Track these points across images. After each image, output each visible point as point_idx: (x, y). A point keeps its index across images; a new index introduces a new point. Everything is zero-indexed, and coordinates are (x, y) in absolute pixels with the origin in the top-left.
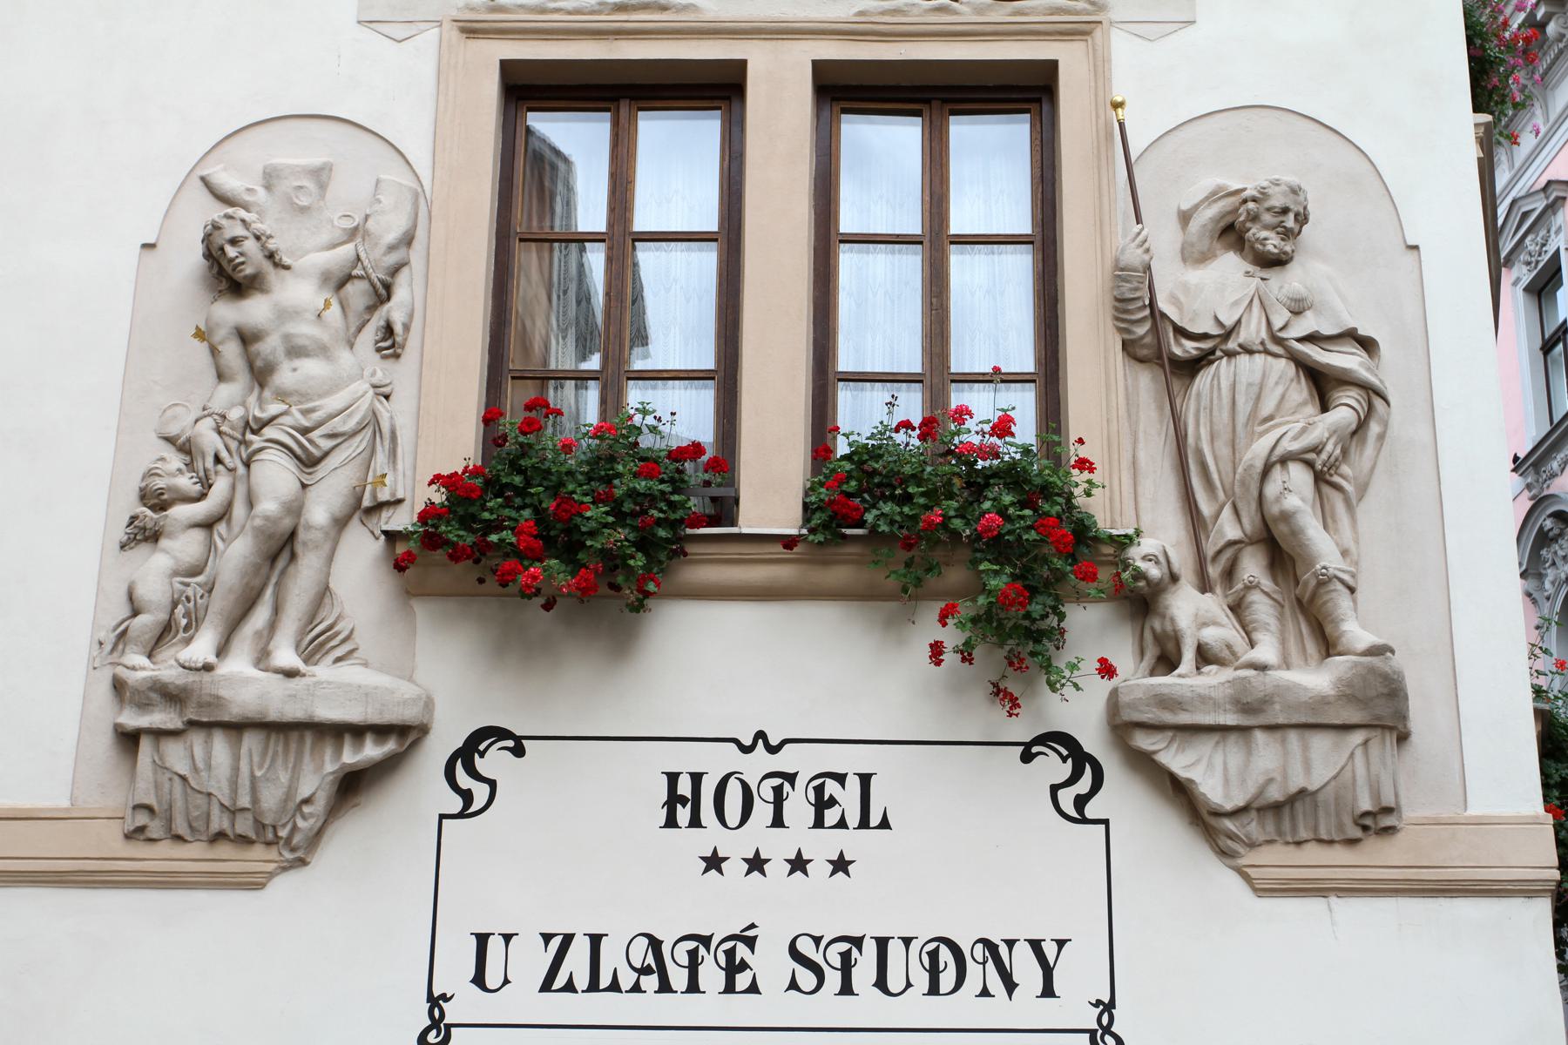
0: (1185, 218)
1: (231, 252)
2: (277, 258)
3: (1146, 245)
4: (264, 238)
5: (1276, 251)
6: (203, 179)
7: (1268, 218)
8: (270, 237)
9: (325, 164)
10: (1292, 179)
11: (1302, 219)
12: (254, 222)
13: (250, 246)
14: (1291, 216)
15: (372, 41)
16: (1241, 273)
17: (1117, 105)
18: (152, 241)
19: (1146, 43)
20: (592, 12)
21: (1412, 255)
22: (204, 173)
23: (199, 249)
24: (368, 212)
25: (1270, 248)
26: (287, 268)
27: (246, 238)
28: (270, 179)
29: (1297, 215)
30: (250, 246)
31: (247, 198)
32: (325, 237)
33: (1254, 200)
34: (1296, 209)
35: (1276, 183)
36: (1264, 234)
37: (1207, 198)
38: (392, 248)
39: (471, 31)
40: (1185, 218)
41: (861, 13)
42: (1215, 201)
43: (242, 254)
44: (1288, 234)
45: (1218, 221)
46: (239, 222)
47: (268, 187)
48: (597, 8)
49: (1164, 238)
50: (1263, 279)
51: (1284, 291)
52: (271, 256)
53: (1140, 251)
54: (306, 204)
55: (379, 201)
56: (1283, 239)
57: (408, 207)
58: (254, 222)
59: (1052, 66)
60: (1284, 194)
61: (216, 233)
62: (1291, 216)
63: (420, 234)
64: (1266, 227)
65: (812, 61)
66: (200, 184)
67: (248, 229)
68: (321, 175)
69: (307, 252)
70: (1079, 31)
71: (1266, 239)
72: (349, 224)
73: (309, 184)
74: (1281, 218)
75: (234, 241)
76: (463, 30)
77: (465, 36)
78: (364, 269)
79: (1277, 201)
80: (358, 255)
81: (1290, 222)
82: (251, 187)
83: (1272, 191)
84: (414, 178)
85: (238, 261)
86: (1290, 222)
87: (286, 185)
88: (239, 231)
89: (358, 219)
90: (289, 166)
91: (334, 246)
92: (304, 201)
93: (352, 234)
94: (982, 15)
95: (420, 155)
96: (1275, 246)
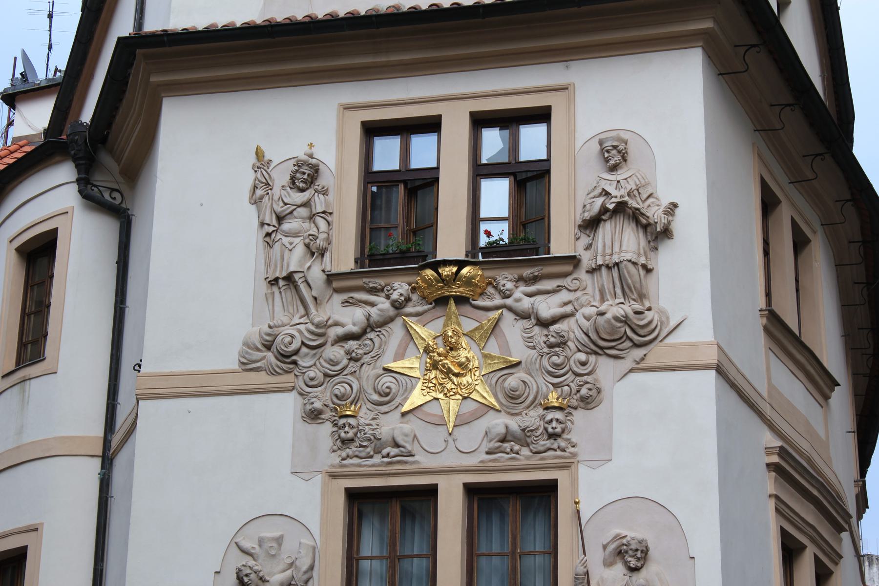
0: (605, 547)
1: (246, 580)
2: (263, 579)
3: (585, 565)
4: (258, 572)
5: (634, 566)
6: (236, 543)
7: (631, 553)
8: (260, 571)
9: (281, 536)
10: (639, 536)
11: (646, 552)
12: (254, 566)
13: (253, 576)
14: (639, 552)
15: (297, 481)
16: (622, 575)
17: (577, 503)
18: (218, 571)
19: (593, 470)
20: (379, 466)
21: (691, 561)
22: (237, 541)
23: (235, 575)
24: (297, 557)
25: (632, 565)
26: (268, 581)
27: (251, 573)
28: (261, 542)
29: (642, 551)
30: (253, 576)
31: (253, 551)
32: (281, 567)
33: (626, 545)
34: (641, 549)
35: (633, 539)
36: (630, 559)
37: (612, 539)
38: (305, 572)
39: (334, 476)
40: (605, 547)
41: (481, 462)
42: (615, 541)
43: (250, 580)
44: (638, 559)
45: (617, 549)
46: (248, 568)
47: (260, 546)
48: (381, 463)
49: (595, 557)
50: (630, 577)
51: (637, 583)
52: (261, 579)
53: (582, 567)
54: (273, 553)
55: (300, 552)
56: (637, 561)
57: (311, 554)
58: (254, 566)
59: (556, 480)
60: (636, 543)
61: (240, 572)
62: (639, 552)
63: (317, 563)
64: (631, 556)
65: (463, 483)
66: (235, 545)
67: (251, 570)
68: (279, 540)
69: (275, 574)
70: (566, 467)
71: (630, 561)
72: (289, 561)
73: (275, 545)
74: (636, 553)
75: (247, 575)
76: (330, 476)
77: (331, 478)
78: (295, 581)
79: (633, 547)
80: (293, 576)
81: (639, 554)
82: (254, 546)
83: (632, 542)
84: (313, 540)
85: (249, 583)
86: (639, 554)
87: (267, 545)
88: (248, 571)
89: (294, 558)
90: (267, 538)
91: (284, 571)
92: (273, 552)
93: (291, 565)
94: (529, 460)
95: (316, 530)
96: (634, 564)
